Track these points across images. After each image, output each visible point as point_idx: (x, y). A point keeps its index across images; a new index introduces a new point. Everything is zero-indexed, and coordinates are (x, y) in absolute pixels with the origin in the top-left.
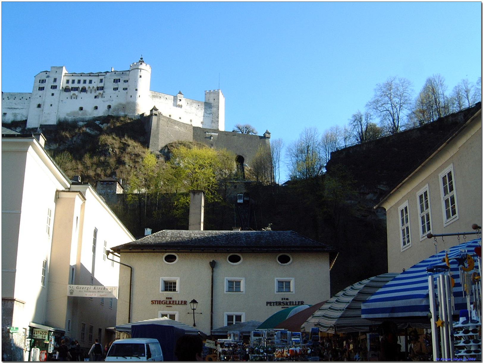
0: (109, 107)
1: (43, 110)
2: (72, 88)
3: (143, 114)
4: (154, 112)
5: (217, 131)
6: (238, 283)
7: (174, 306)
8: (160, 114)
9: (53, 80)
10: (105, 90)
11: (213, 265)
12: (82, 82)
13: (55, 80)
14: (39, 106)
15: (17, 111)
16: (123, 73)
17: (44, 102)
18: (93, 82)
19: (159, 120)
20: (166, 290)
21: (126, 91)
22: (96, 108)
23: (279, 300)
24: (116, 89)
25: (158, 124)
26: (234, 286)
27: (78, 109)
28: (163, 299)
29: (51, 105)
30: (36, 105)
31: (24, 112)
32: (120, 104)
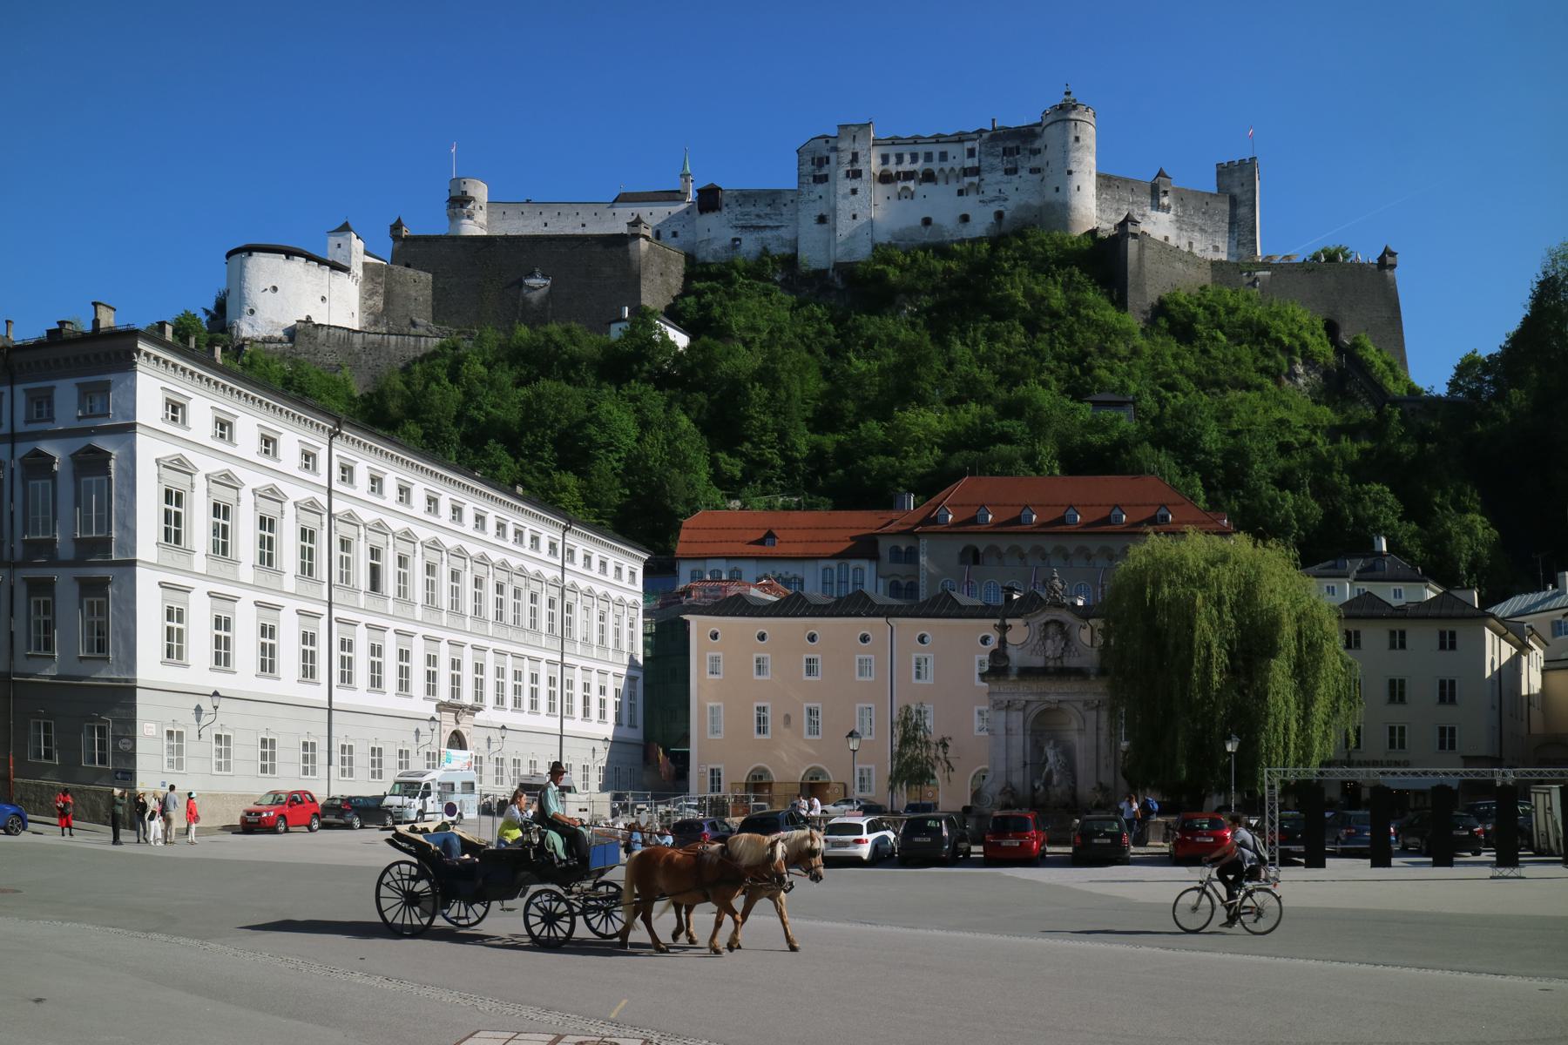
0: (999, 215)
3: (1093, 233)
4: (1131, 229)
10: (985, 176)
14: (822, 219)
15: (768, 234)
17: (834, 210)
18: (950, 157)
19: (1142, 248)
21: (1037, 177)
24: (1011, 171)
25: (1140, 259)
30: (813, 221)
31: (785, 233)
32: (1028, 207)
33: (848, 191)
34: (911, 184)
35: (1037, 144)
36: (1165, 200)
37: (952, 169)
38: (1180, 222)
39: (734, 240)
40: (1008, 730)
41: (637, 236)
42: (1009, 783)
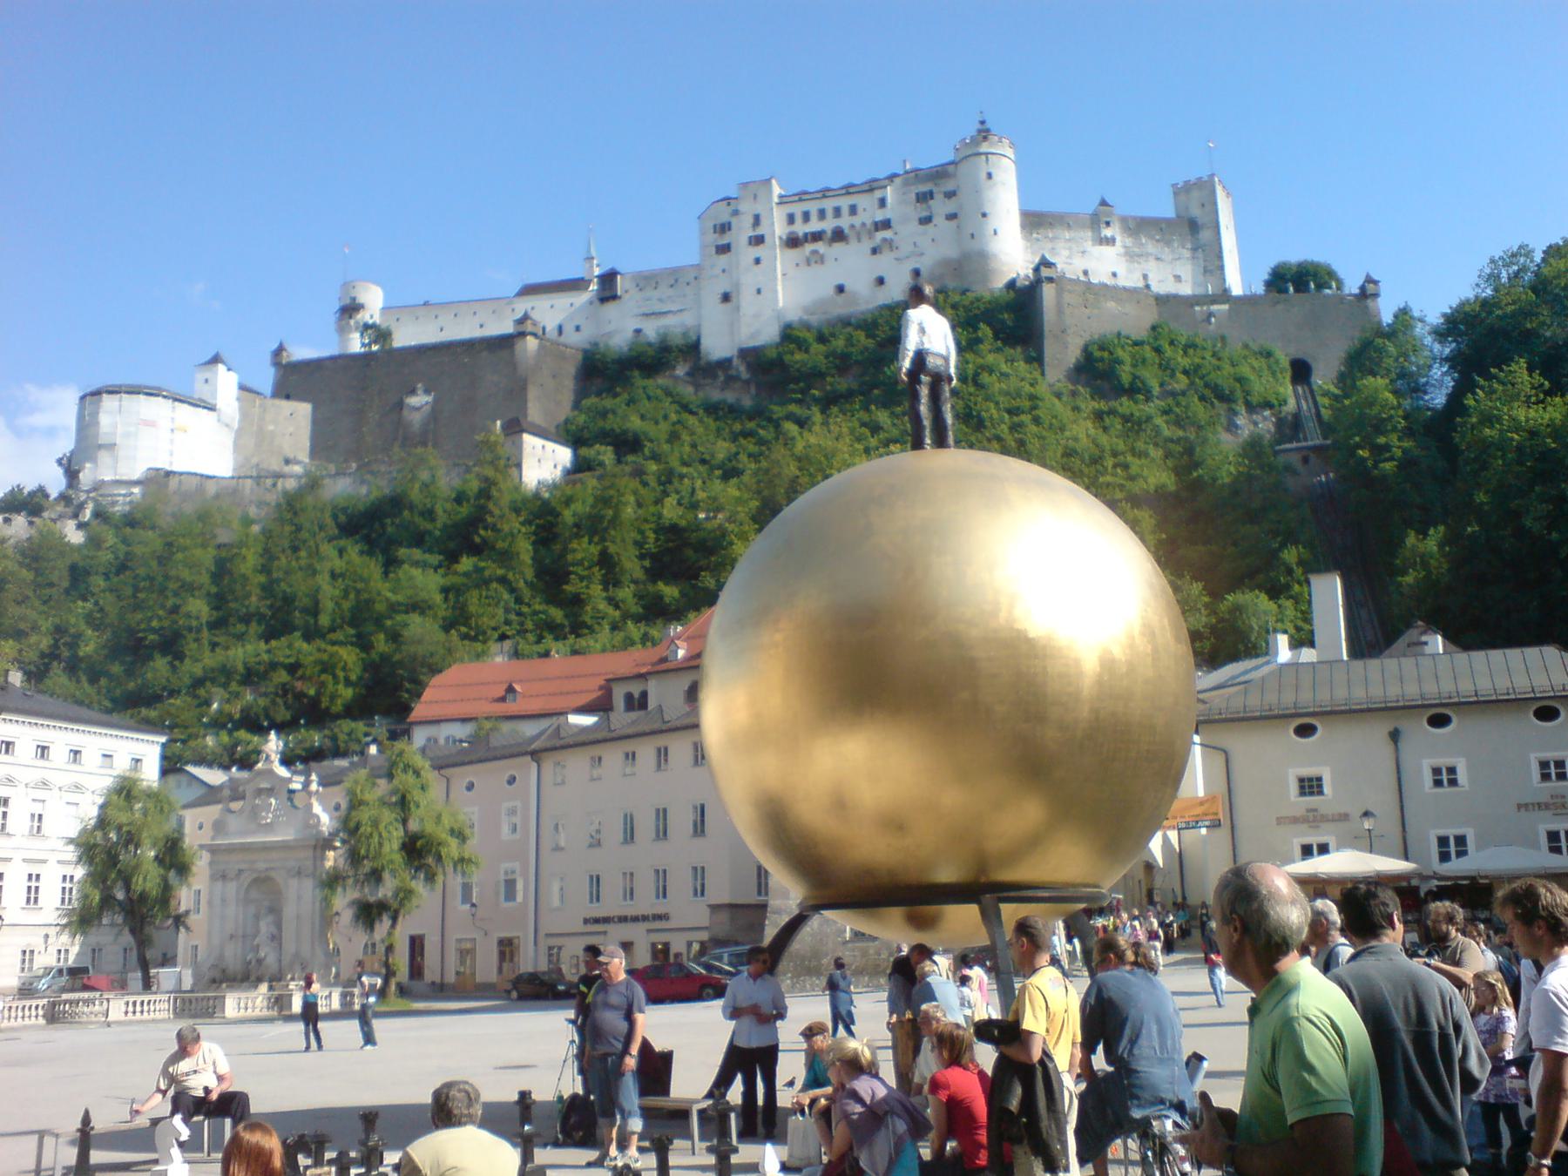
0: (917, 273)
1: (738, 308)
2: (806, 235)
4: (1045, 272)
5: (1224, 295)
6: (1452, 770)
7: (1325, 826)
8: (1063, 277)
9: (751, 220)
11: (1395, 736)
12: (829, 213)
13: (757, 220)
14: (726, 298)
16: (940, 174)
17: (737, 285)
18: (860, 209)
20: (1302, 793)
21: (953, 224)
22: (881, 281)
23: (1544, 798)
24: (926, 221)
26: (1444, 777)
27: (830, 291)
28: (1300, 812)
29: (759, 291)
31: (688, 319)
33: (751, 260)
34: (820, 246)
35: (949, 185)
36: (1108, 232)
37: (864, 224)
38: (1130, 256)
39: (638, 331)
40: (223, 900)
41: (522, 334)
42: (221, 957)
